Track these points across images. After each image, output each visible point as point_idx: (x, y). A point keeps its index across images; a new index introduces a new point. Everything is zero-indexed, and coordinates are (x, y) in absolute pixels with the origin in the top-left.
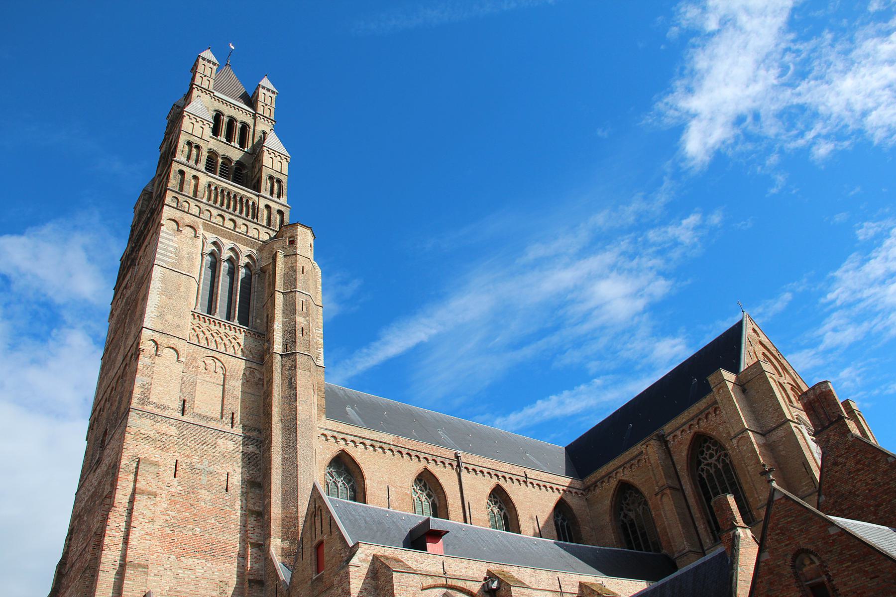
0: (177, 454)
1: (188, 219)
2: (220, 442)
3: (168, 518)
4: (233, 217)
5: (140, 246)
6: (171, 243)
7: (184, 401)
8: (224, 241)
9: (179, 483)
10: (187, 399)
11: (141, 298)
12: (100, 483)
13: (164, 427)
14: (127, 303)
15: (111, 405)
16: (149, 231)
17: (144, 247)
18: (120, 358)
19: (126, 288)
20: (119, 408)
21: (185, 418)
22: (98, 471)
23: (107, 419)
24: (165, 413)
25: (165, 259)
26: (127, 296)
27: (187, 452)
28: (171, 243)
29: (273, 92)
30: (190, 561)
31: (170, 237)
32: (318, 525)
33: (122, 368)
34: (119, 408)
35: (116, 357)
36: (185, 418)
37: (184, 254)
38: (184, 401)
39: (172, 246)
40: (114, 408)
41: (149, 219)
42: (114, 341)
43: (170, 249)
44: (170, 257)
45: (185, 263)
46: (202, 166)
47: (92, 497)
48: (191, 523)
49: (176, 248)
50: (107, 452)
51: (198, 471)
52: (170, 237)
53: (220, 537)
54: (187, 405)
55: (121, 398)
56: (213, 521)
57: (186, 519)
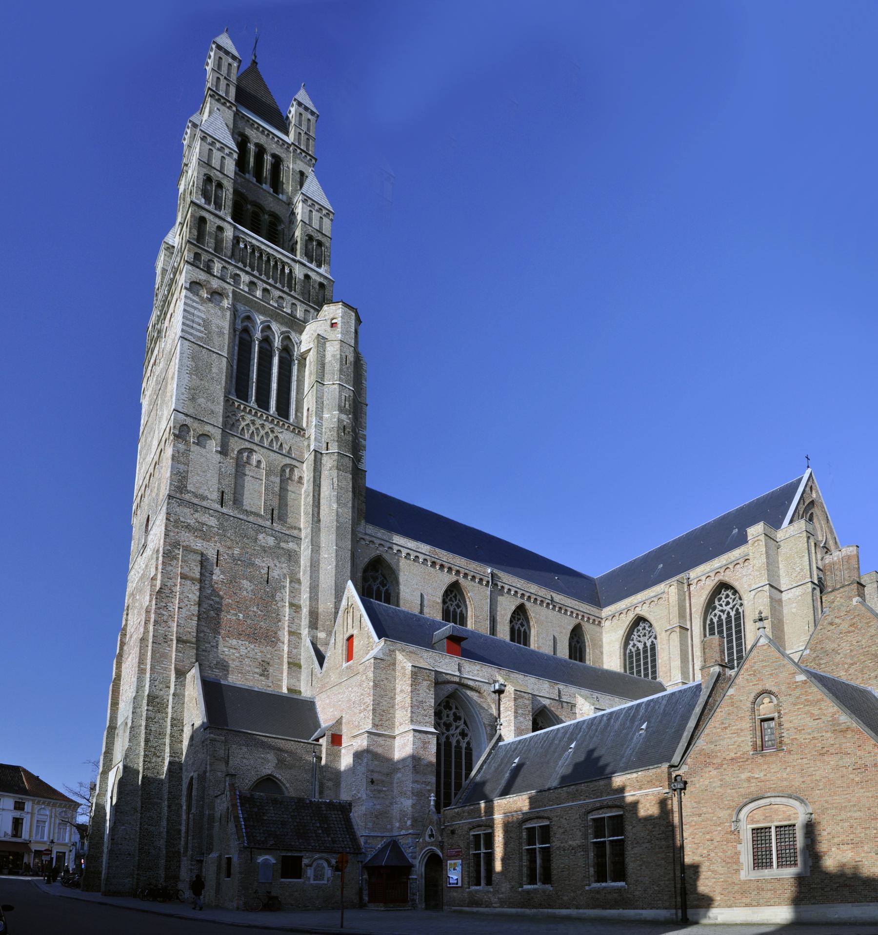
3: (211, 602)
5: (166, 314)
7: (223, 492)
9: (222, 573)
11: (170, 377)
12: (147, 566)
14: (157, 383)
15: (151, 491)
16: (173, 295)
17: (168, 316)
18: (155, 443)
19: (155, 364)
20: (158, 495)
22: (144, 555)
23: (149, 505)
24: (204, 504)
25: (192, 331)
26: (157, 373)
29: (313, 113)
30: (234, 642)
32: (350, 621)
33: (158, 454)
34: (158, 495)
35: (151, 441)
38: (223, 492)
40: (154, 495)
41: (172, 280)
42: (149, 424)
43: (197, 320)
46: (226, 213)
47: (141, 578)
48: (233, 609)
50: (150, 537)
54: (226, 497)
55: (159, 485)
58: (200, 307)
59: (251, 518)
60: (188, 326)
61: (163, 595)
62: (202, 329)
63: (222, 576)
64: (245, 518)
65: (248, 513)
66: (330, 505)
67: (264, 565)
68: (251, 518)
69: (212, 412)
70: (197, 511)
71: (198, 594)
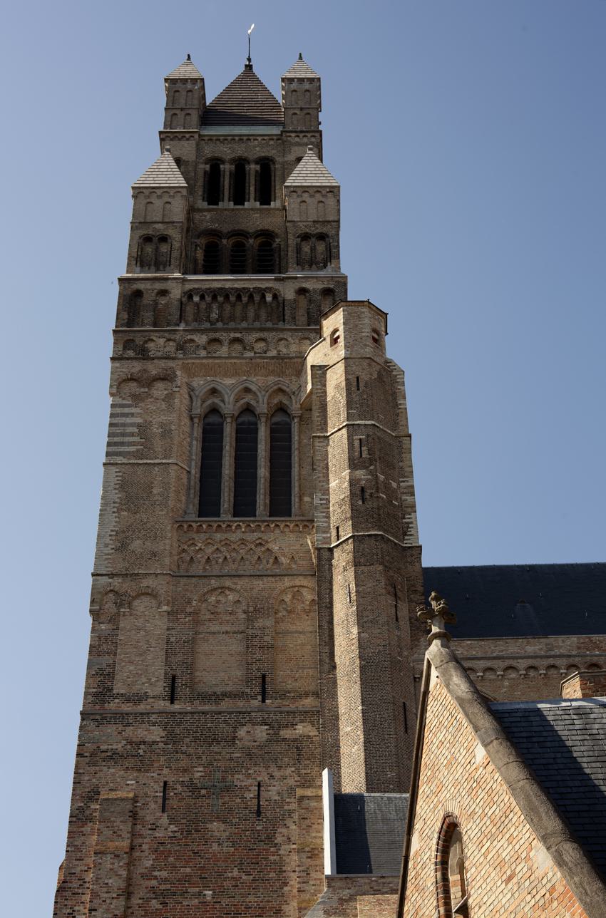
0: (165, 771)
1: (153, 369)
2: (242, 732)
3: (154, 883)
4: (238, 335)
6: (129, 420)
7: (174, 678)
8: (229, 381)
9: (172, 820)
10: (178, 673)
13: (141, 733)
21: (177, 707)
24: (142, 707)
27: (184, 763)
28: (129, 420)
31: (126, 410)
36: (177, 707)
37: (156, 430)
39: (132, 425)
44: (130, 444)
45: (158, 445)
49: (139, 426)
51: (203, 792)
52: (126, 410)
53: (251, 898)
54: (179, 683)
56: (236, 873)
57: (187, 879)
58: (133, 410)
59: (225, 705)
60: (116, 444)
61: (68, 894)
62: (136, 439)
63: (172, 828)
64: (214, 708)
65: (217, 697)
66: (349, 632)
67: (250, 781)
68: (225, 705)
69: (154, 554)
70: (129, 725)
71: (124, 873)
